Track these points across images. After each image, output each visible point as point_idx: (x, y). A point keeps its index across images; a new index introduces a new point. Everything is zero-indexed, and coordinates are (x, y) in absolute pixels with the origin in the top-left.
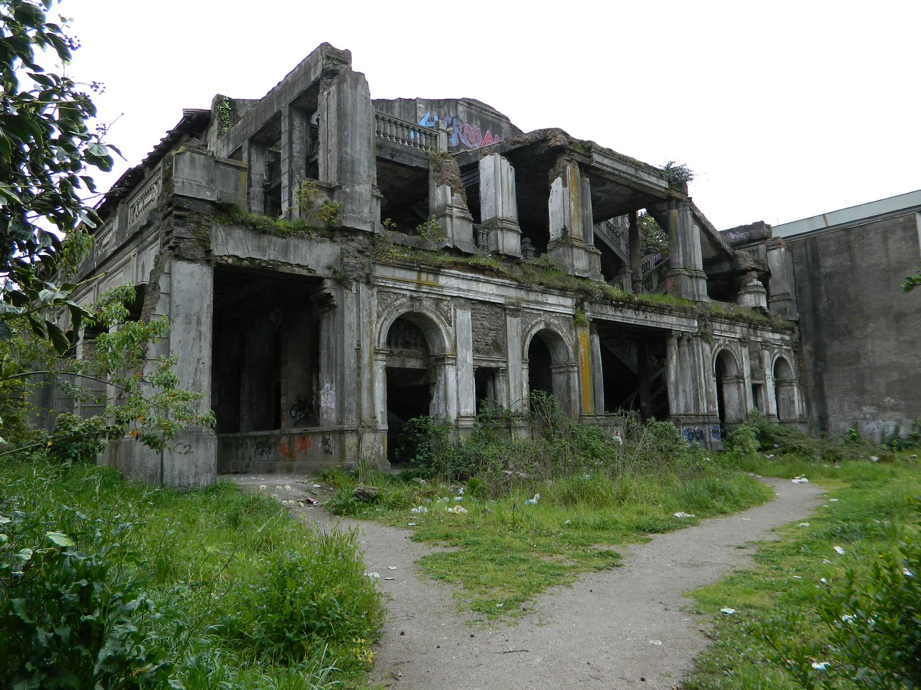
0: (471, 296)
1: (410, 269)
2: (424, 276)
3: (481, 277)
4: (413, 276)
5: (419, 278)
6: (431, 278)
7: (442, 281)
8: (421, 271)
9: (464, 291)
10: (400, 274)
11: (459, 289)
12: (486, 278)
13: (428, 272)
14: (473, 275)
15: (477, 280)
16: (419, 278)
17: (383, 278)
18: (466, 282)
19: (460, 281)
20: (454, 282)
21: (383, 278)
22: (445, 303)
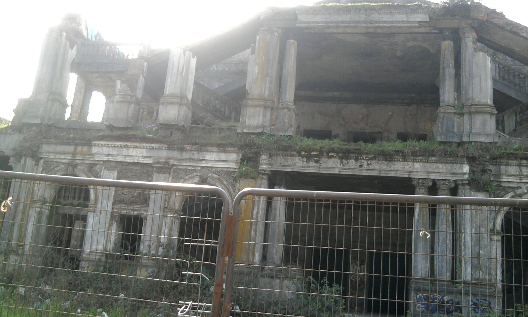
0: (120, 159)
1: (68, 144)
2: (79, 148)
3: (129, 144)
4: (71, 148)
5: (75, 149)
6: (85, 149)
7: (95, 150)
8: (77, 145)
9: (112, 155)
10: (60, 148)
11: (109, 155)
12: (135, 144)
13: (83, 145)
14: (122, 143)
15: (125, 146)
16: (75, 149)
17: (46, 152)
18: (117, 149)
19: (111, 149)
20: (105, 150)
21: (46, 152)
22: (98, 166)
